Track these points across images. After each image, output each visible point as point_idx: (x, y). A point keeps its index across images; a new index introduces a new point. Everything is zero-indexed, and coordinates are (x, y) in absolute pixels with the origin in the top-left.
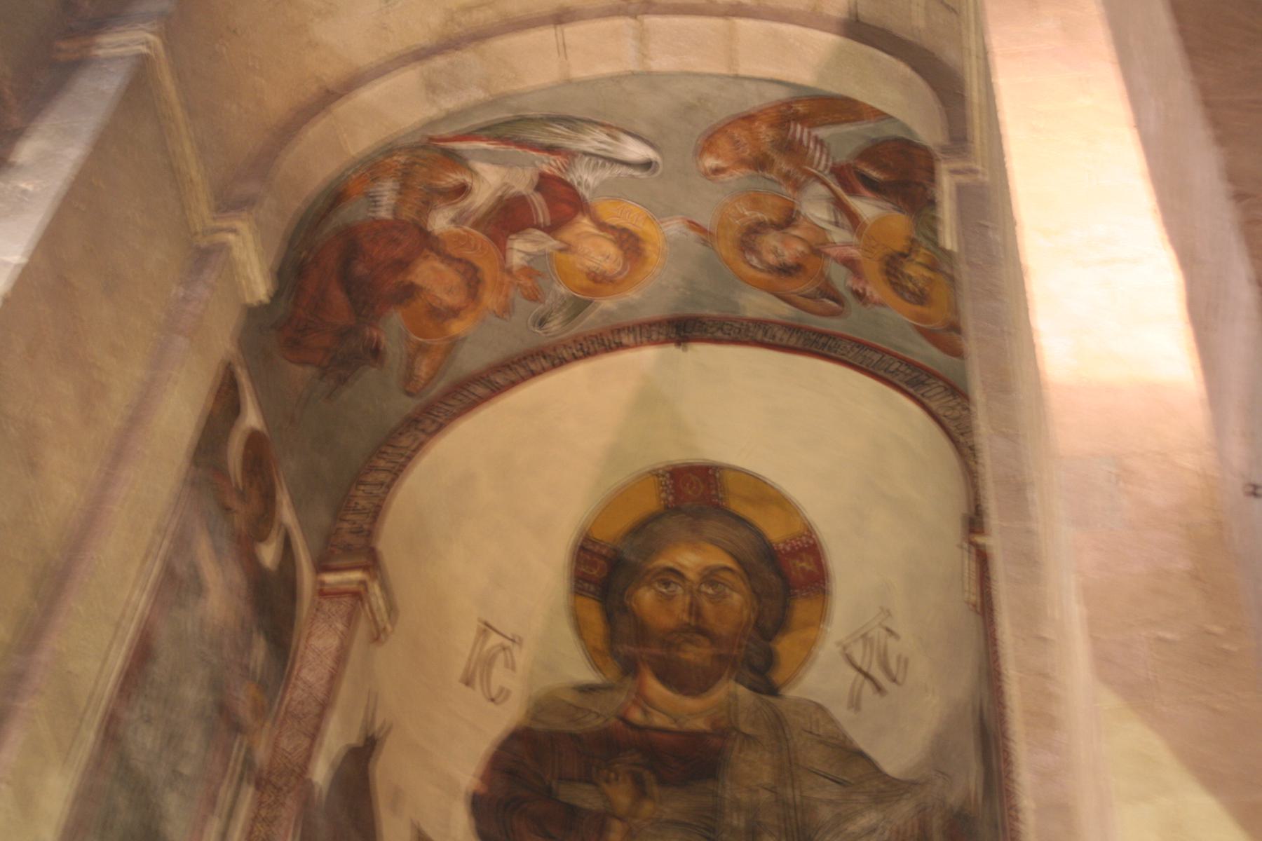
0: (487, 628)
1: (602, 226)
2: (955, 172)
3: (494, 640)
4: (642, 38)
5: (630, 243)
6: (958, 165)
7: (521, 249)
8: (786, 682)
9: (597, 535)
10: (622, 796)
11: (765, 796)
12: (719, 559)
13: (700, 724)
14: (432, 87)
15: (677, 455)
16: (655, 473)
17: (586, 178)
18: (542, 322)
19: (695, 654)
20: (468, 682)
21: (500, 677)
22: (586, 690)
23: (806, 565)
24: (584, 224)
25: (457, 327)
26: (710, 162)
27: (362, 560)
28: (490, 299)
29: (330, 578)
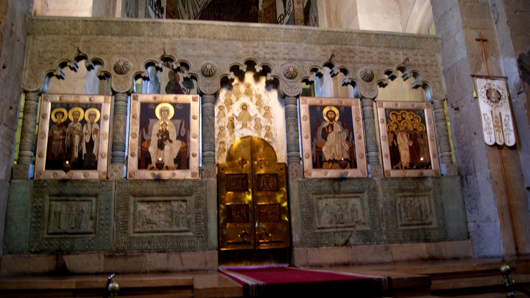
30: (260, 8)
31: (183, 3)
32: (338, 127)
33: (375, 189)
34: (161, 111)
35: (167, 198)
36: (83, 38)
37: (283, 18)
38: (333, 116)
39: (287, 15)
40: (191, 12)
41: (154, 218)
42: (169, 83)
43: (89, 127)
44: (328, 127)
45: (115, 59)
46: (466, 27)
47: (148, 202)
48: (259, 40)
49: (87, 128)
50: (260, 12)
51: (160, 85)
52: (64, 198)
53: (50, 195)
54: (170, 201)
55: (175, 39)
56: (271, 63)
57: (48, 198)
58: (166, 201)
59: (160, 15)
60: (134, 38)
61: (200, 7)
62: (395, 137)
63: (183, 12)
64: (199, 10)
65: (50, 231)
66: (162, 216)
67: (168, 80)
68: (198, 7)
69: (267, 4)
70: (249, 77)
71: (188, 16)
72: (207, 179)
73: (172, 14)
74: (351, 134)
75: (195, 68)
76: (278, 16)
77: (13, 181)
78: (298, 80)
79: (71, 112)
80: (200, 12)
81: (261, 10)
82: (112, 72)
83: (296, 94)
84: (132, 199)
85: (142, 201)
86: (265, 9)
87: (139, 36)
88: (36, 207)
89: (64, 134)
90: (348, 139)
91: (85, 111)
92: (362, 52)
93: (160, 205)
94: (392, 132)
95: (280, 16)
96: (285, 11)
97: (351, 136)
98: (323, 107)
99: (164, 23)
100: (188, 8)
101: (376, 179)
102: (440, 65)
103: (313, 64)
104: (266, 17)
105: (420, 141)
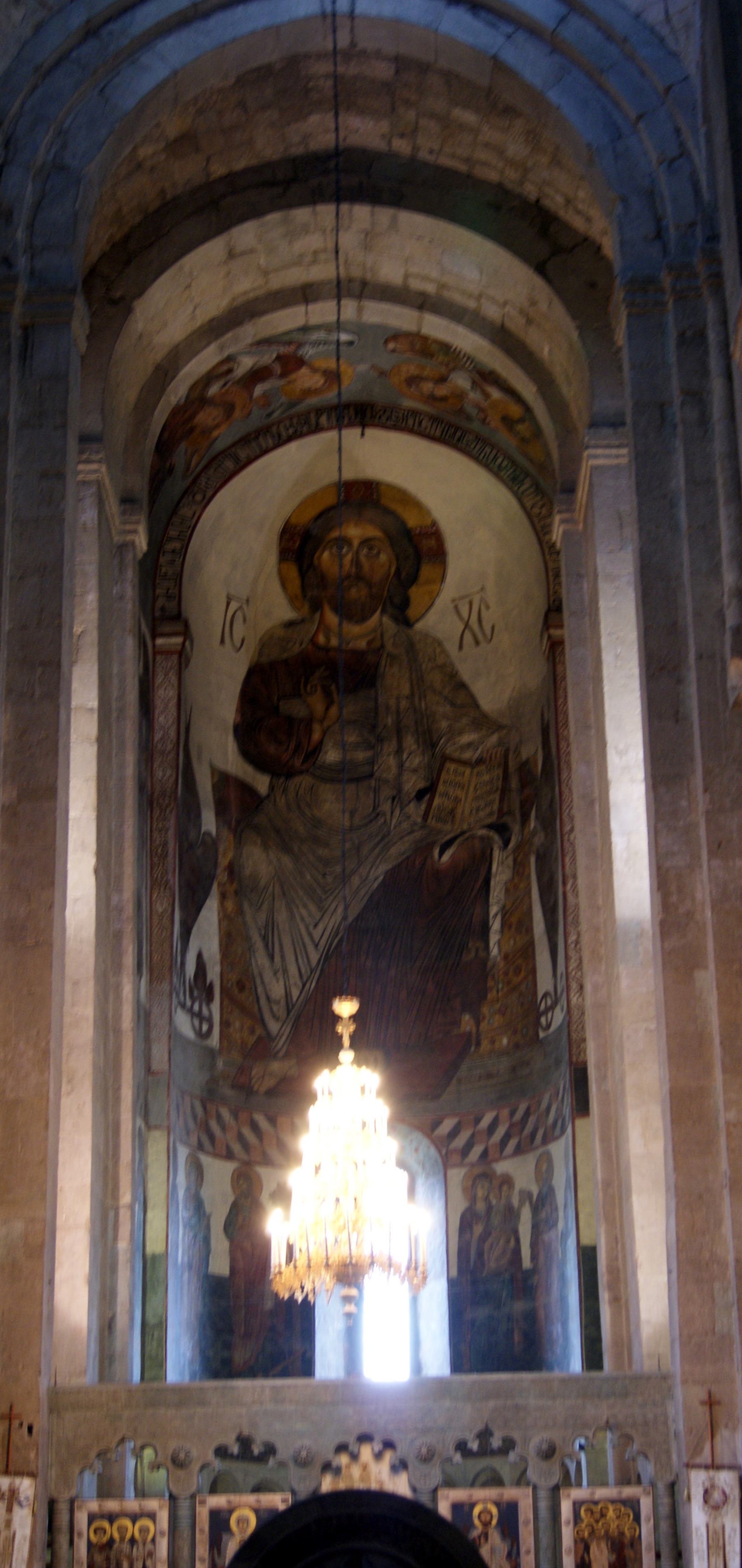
1: (315, 370)
2: (563, 521)
3: (234, 606)
4: (360, 310)
6: (566, 516)
7: (259, 390)
8: (418, 620)
9: (293, 521)
10: (317, 703)
12: (372, 532)
13: (362, 644)
14: (221, 348)
17: (308, 352)
18: (269, 415)
19: (357, 593)
20: (222, 641)
21: (239, 630)
23: (433, 542)
24: (304, 370)
25: (215, 434)
26: (391, 346)
27: (179, 627)
28: (237, 413)
29: (160, 641)
30: (494, 951)
32: (495, 1537)
34: (238, 1521)
37: (552, 1008)
38: (488, 1518)
40: (293, 970)
43: (141, 1548)
44: (479, 1537)
49: (138, 1549)
50: (494, 965)
51: (209, 1220)
56: (396, 1437)
59: (205, 1011)
62: (587, 1548)
63: (268, 975)
64: (314, 957)
67: (231, 1199)
68: (310, 948)
69: (512, 942)
70: (366, 1452)
71: (282, 983)
74: (515, 1548)
75: (284, 1452)
76: (540, 994)
81: (496, 957)
83: (433, 1486)
86: (506, 957)
89: (108, 1559)
90: (509, 1555)
91: (134, 1523)
94: (583, 1540)
97: (515, 1551)
98: (472, 1505)
100: (283, 957)
103: (459, 1435)
104: (509, 982)
105: (629, 1553)
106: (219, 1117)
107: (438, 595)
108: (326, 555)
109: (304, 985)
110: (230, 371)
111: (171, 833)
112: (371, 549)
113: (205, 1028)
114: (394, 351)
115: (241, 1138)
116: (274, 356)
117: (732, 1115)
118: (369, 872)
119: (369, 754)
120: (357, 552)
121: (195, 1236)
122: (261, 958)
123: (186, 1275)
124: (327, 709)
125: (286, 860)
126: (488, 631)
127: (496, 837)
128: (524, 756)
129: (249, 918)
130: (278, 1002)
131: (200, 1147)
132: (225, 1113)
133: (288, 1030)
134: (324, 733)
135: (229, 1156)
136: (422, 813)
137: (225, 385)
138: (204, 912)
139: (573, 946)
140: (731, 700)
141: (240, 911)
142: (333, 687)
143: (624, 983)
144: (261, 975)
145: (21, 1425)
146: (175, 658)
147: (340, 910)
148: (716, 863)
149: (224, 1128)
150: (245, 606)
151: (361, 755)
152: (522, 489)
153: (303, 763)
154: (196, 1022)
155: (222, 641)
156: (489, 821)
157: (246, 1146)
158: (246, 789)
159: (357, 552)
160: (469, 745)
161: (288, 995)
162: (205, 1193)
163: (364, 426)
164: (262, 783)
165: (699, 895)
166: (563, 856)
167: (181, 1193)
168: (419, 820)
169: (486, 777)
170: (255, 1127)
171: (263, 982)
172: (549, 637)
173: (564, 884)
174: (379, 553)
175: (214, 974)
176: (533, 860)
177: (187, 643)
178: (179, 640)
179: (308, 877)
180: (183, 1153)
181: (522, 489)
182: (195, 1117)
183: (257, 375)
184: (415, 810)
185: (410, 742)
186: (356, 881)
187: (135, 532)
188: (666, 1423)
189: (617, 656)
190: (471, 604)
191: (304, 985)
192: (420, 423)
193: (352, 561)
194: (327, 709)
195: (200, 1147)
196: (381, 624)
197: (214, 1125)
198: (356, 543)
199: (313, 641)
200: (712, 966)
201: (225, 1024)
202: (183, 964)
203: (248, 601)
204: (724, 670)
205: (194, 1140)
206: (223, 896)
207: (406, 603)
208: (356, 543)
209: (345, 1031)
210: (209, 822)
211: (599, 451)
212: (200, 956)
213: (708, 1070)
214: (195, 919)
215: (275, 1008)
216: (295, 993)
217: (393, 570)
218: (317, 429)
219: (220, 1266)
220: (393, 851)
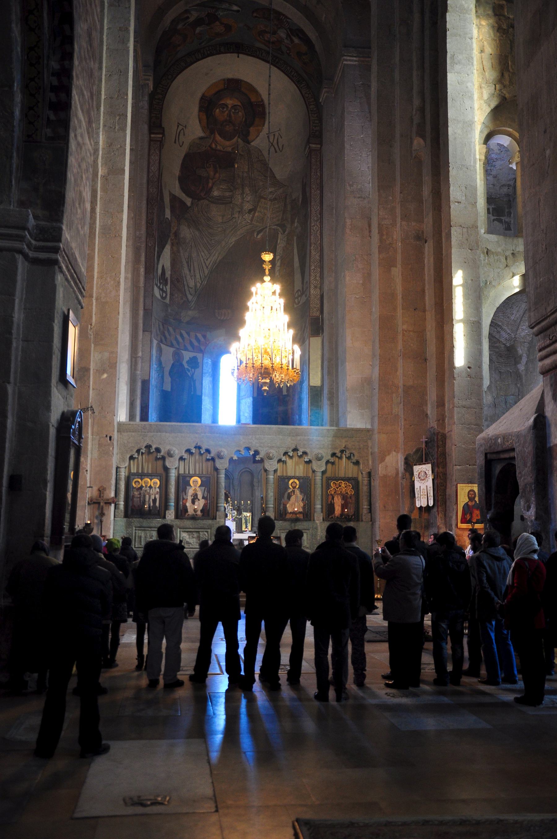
0: (179, 124)
3: (180, 127)
5: (228, 28)
7: (198, 30)
8: (252, 141)
11: (245, 175)
13: (230, 149)
15: (230, 76)
16: (224, 80)
17: (221, 13)
18: (200, 44)
20: (175, 142)
22: (201, 138)
24: (217, 23)
26: (255, 15)
29: (152, 136)
31: (188, 266)
33: (316, 528)
35: (198, 530)
36: (150, 434)
39: (304, 296)
40: (198, 276)
41: (191, 541)
42: (173, 365)
45: (168, 447)
46: (380, 432)
47: (187, 532)
48: (252, 435)
52: (143, 529)
53: (135, 527)
54: (199, 532)
55: (202, 435)
56: (259, 449)
57: (134, 528)
58: (197, 532)
59: (165, 289)
60: (179, 434)
61: (207, 267)
63: (188, 277)
64: (206, 272)
65: (136, 546)
66: (194, 539)
67: (172, 362)
68: (205, 267)
71: (193, 280)
72: (219, 520)
73: (176, 282)
77: (116, 519)
78: (275, 460)
79: (143, 481)
80: (208, 274)
82: (166, 456)
84: (179, 530)
85: (184, 531)
87: (181, 433)
88: (128, 533)
92: (318, 441)
93: (194, 534)
95: (297, 291)
96: (303, 288)
99: (196, 426)
100: (194, 271)
101: (317, 522)
102: (369, 449)
106: (168, 330)
107: (261, 132)
108: (218, 110)
109: (202, 283)
110: (188, 18)
111: (155, 214)
112: (235, 110)
113: (164, 295)
114: (256, 17)
115: (176, 339)
116: (206, 13)
117: (405, 327)
118: (228, 241)
119: (231, 193)
120: (230, 111)
121: (159, 375)
122: (186, 271)
123: (155, 390)
124: (215, 174)
125: (197, 233)
126: (281, 147)
127: (280, 230)
128: (294, 197)
129: (182, 254)
130: (191, 288)
131: (161, 341)
132: (171, 329)
133: (195, 300)
134: (213, 184)
135: (172, 346)
136: (250, 218)
137: (184, 25)
138: (165, 250)
139: (312, 271)
140: (414, 155)
141: (179, 251)
142: (217, 166)
143: (348, 278)
144: (186, 277)
145: (107, 436)
146: (159, 143)
147: (216, 254)
148: (404, 223)
149: (170, 335)
150: (184, 129)
151: (227, 194)
152: (301, 86)
153: (204, 195)
154: (161, 292)
155: (175, 142)
156: (277, 223)
157: (178, 342)
158: (183, 203)
159: (230, 111)
160: (271, 192)
161: (196, 286)
162: (163, 359)
163: (238, 53)
164: (188, 201)
165: (395, 237)
166: (311, 235)
167: (154, 358)
168: (249, 221)
169: (277, 206)
170: (181, 335)
171: (186, 280)
172: (310, 147)
173: (310, 246)
174: (238, 112)
175: (168, 274)
176: (295, 238)
177: (163, 138)
178: (161, 136)
179: (205, 240)
180: (155, 342)
181: (301, 86)
182: (160, 329)
183: (199, 22)
184: (248, 217)
185: (247, 190)
186: (223, 243)
187: (148, 80)
188: (367, 449)
189: (351, 145)
190: (274, 135)
191: (202, 283)
192: (262, 54)
193: (228, 114)
194: (215, 174)
195: (161, 341)
196: (238, 142)
197: (166, 333)
198: (230, 106)
199: (210, 146)
200: (399, 266)
201: (171, 294)
202: (157, 269)
203: (185, 127)
204: (412, 143)
205: (159, 339)
206: (172, 245)
207: (248, 133)
208: (230, 106)
209: (267, 267)
210: (168, 214)
211: (348, 58)
212: (163, 266)
213: (395, 309)
214: (162, 252)
215: (190, 289)
216: (198, 285)
217: (244, 119)
218: (220, 53)
219: (168, 387)
220: (239, 233)
